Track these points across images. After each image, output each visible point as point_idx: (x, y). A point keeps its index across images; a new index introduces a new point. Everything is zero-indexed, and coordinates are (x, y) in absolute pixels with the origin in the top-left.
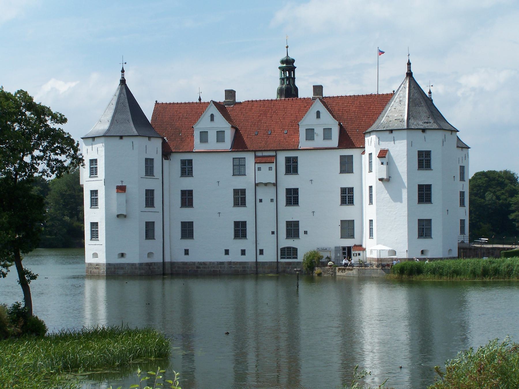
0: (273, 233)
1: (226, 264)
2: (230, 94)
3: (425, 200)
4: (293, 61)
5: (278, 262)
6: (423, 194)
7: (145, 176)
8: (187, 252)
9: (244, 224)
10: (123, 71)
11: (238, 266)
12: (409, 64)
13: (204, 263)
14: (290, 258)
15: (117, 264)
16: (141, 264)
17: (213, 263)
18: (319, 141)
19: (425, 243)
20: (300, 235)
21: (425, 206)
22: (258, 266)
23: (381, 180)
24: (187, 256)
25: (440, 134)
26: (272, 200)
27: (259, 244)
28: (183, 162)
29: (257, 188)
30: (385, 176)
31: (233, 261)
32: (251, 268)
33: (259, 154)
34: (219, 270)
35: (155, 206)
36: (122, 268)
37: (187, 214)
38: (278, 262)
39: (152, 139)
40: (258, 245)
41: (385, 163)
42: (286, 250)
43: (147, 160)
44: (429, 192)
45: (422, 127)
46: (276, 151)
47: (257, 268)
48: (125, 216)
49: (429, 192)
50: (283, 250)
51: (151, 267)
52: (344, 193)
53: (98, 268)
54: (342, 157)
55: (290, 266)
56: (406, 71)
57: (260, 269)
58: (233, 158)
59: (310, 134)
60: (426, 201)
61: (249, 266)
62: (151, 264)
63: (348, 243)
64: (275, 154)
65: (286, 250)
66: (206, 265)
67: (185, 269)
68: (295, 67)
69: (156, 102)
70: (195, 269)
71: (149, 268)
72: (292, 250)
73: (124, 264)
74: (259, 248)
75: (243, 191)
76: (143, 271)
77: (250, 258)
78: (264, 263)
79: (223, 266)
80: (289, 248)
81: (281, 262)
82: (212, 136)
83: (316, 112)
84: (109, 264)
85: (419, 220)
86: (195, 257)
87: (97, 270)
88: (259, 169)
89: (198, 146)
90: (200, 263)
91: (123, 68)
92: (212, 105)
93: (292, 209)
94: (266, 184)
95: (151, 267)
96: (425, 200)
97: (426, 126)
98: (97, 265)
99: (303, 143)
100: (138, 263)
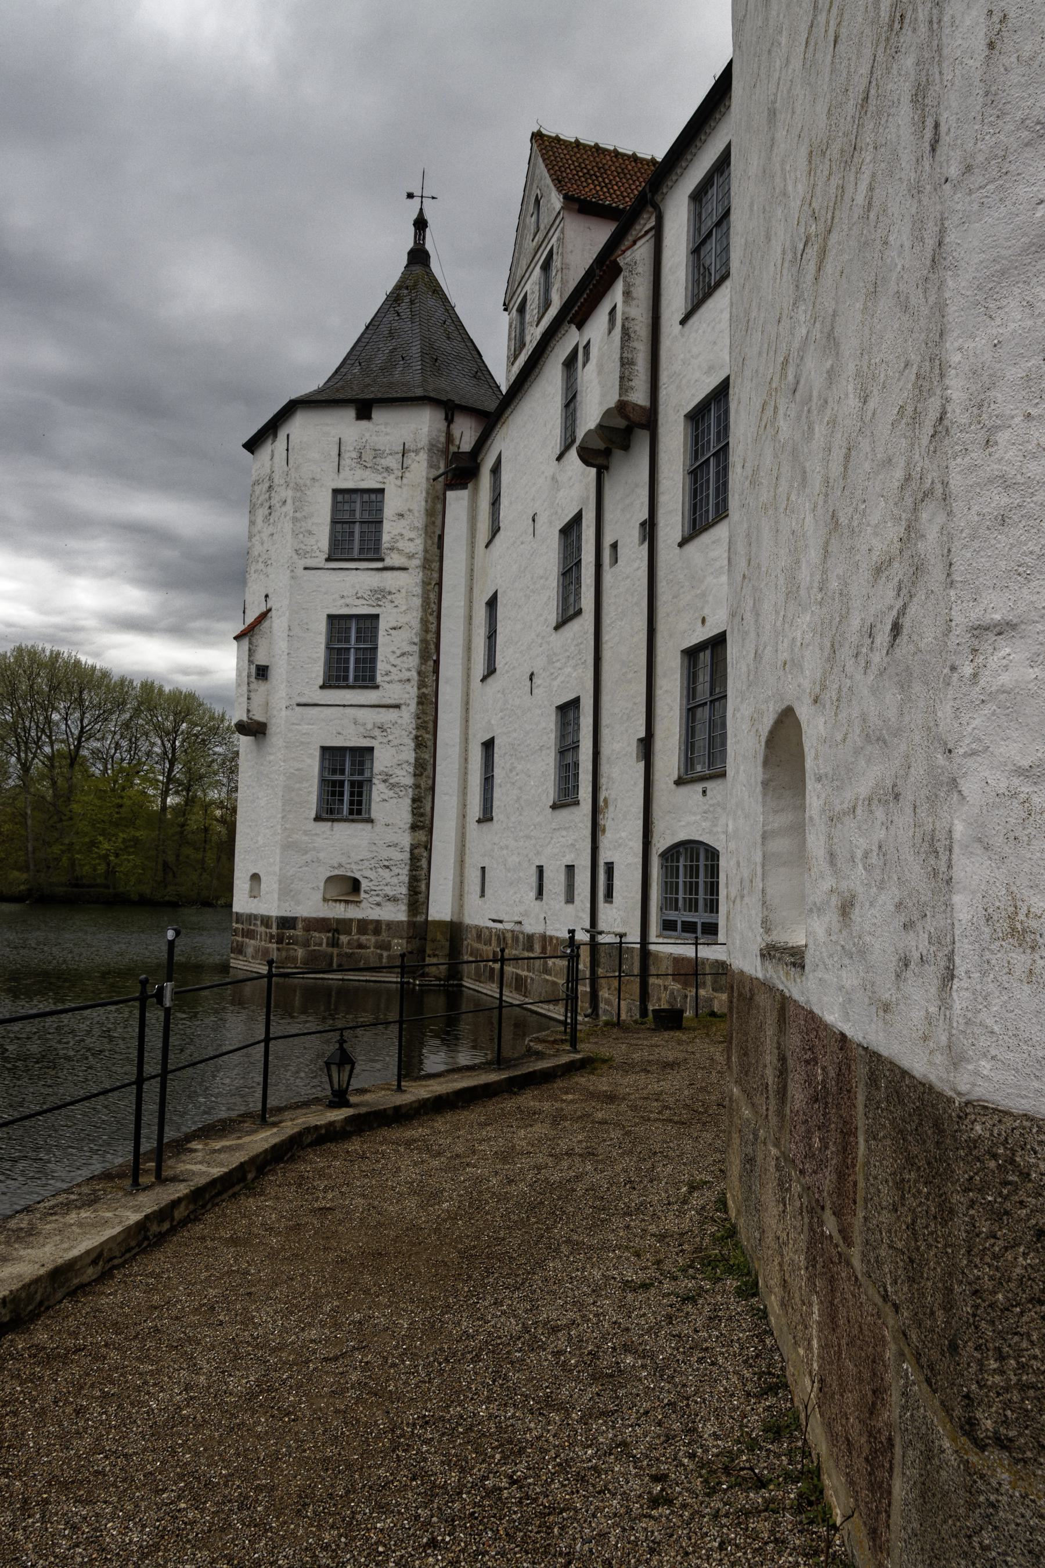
10: (421, 224)
16: (286, 923)
35: (379, 679)
51: (344, 939)
71: (334, 943)
81: (656, 955)
91: (421, 209)
95: (344, 939)
100: (277, 917)
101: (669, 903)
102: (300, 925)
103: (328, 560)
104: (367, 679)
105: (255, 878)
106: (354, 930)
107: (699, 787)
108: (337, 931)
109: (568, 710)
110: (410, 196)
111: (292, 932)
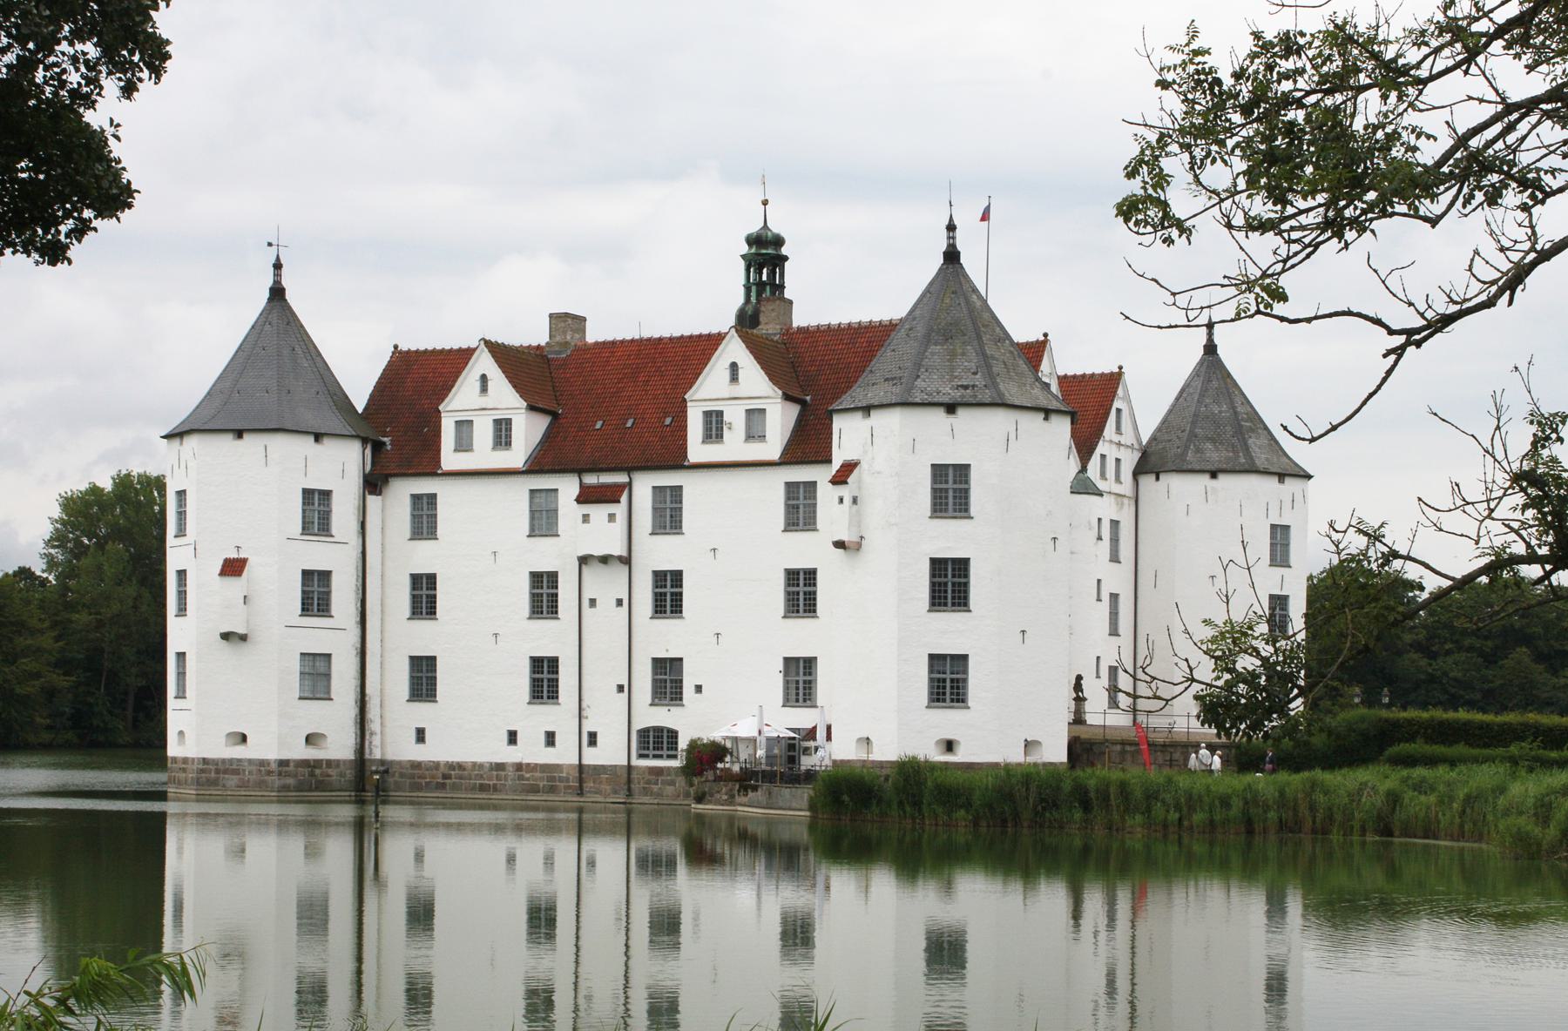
0: (620, 688)
1: (511, 769)
2: (567, 323)
3: (949, 600)
4: (778, 242)
5: (629, 767)
6: (946, 584)
7: (302, 534)
8: (421, 735)
9: (553, 663)
11: (538, 774)
12: (951, 227)
13: (460, 766)
14: (660, 757)
15: (224, 761)
16: (283, 763)
17: (481, 766)
18: (734, 446)
19: (948, 721)
20: (684, 696)
21: (949, 620)
22: (583, 776)
23: (840, 545)
24: (421, 746)
25: (996, 422)
26: (619, 602)
27: (587, 718)
28: (416, 499)
29: (584, 567)
30: (845, 537)
31: (525, 761)
32: (567, 780)
33: (591, 479)
34: (495, 785)
35: (333, 613)
36: (236, 772)
37: (423, 638)
38: (629, 767)
39: (326, 441)
40: (584, 722)
41: (847, 500)
42: (651, 734)
43: (308, 494)
44: (963, 580)
45: (946, 399)
46: (630, 470)
47: (581, 781)
48: (243, 638)
49: (963, 580)
50: (644, 733)
51: (318, 771)
52: (793, 585)
53: (184, 770)
54: (791, 487)
55: (660, 779)
56: (944, 247)
57: (589, 785)
58: (532, 491)
59: (715, 426)
60: (953, 604)
61: (564, 775)
62: (317, 763)
63: (802, 718)
64: (627, 480)
65: (651, 734)
66: (464, 769)
67: (417, 780)
68: (786, 258)
69: (396, 347)
70: (440, 780)
71: (312, 774)
72: (665, 734)
73: (239, 760)
74: (588, 727)
75: (553, 577)
76: (291, 781)
77: (564, 755)
78: (599, 770)
79: (503, 773)
80: (659, 730)
81: (637, 767)
82: (483, 432)
83: (727, 365)
84: (204, 759)
85: (930, 655)
86: (435, 752)
87: (184, 775)
88: (586, 518)
89: (450, 459)
90: (452, 766)
92: (483, 351)
93: (667, 625)
94: (605, 560)
95: (318, 771)
96: (949, 600)
97: (957, 395)
98: (185, 760)
99: (697, 450)
101: (639, 748)
102: (292, 764)
105: (181, 733)
108: (314, 767)
111: (287, 768)
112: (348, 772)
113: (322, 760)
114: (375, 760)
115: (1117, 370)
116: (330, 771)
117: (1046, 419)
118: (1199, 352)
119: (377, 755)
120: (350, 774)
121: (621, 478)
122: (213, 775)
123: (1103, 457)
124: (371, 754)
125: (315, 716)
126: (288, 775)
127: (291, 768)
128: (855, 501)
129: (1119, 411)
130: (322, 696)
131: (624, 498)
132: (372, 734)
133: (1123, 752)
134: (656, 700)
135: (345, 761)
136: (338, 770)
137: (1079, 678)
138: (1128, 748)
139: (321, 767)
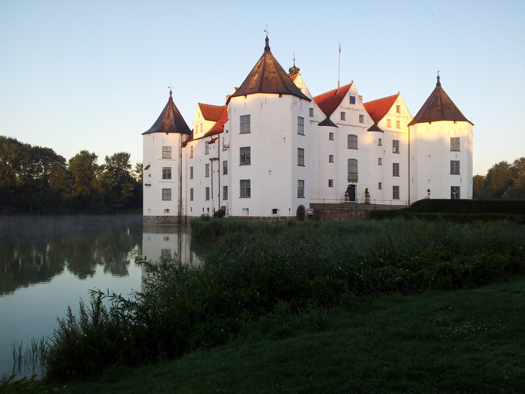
10: (171, 93)
16: (157, 217)
35: (172, 178)
36: (149, 219)
48: (150, 185)
51: (167, 219)
62: (167, 217)
71: (166, 220)
73: (150, 216)
76: (160, 221)
94: (215, 159)
95: (167, 219)
102: (160, 217)
103: (163, 158)
104: (169, 177)
106: (169, 217)
107: (225, 200)
109: (208, 189)
110: (169, 87)
112: (176, 219)
113: (169, 216)
114: (184, 216)
115: (398, 93)
116: (171, 219)
117: (280, 96)
118: (435, 86)
119: (184, 215)
120: (177, 219)
121: (216, 136)
122: (146, 220)
123: (389, 120)
124: (183, 214)
125: (167, 204)
126: (159, 220)
127: (160, 218)
128: (227, 132)
129: (398, 107)
130: (169, 199)
131: (217, 141)
132: (183, 209)
133: (331, 213)
134: (225, 198)
135: (175, 216)
136: (173, 218)
137: (367, 189)
138: (333, 211)
139: (168, 218)
